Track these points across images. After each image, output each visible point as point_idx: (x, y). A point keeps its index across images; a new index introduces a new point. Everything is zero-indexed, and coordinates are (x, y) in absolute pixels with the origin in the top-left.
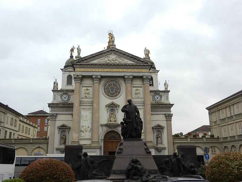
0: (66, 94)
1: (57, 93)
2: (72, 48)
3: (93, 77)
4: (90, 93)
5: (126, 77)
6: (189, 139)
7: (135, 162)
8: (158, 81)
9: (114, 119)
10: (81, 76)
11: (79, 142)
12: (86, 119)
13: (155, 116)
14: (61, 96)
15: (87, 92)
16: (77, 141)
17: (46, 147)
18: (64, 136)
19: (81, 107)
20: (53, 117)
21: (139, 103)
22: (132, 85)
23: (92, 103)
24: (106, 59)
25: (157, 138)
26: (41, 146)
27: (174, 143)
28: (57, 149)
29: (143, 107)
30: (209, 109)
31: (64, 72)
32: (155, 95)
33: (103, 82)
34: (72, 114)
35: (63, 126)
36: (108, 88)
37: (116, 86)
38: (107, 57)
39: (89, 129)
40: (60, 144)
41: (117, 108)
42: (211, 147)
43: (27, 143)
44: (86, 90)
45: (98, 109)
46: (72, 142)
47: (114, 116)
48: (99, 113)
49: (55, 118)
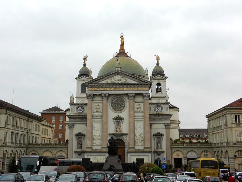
0: (81, 107)
2: (85, 57)
3: (102, 95)
4: (100, 108)
5: (129, 95)
6: (185, 145)
7: (112, 166)
8: (165, 86)
9: (119, 130)
10: (92, 95)
11: (92, 147)
12: (97, 129)
13: (157, 125)
14: (77, 109)
15: (98, 107)
16: (90, 147)
17: (67, 150)
18: (81, 142)
19: (93, 120)
21: (140, 116)
22: (135, 101)
23: (102, 116)
24: (113, 80)
25: (157, 144)
26: (62, 149)
28: (75, 152)
29: (143, 119)
30: (208, 117)
31: (78, 81)
33: (110, 99)
34: (86, 124)
35: (80, 133)
36: (114, 104)
37: (120, 101)
38: (114, 78)
39: (100, 137)
40: (77, 149)
41: (122, 120)
42: (204, 151)
43: (52, 147)
44: (97, 105)
45: (107, 122)
46: (87, 147)
47: (120, 127)
48: (107, 125)
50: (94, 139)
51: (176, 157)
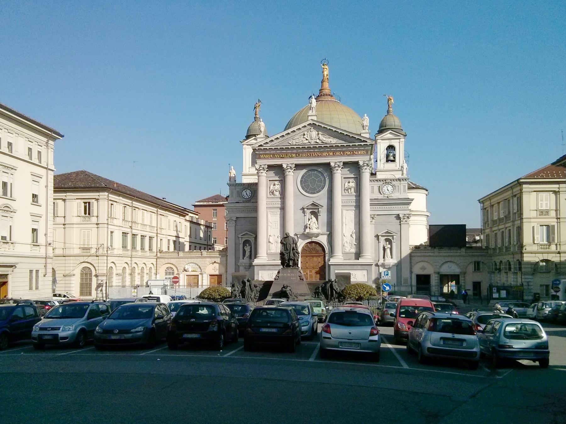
32: (383, 186)
36: (305, 182)
50: (269, 242)
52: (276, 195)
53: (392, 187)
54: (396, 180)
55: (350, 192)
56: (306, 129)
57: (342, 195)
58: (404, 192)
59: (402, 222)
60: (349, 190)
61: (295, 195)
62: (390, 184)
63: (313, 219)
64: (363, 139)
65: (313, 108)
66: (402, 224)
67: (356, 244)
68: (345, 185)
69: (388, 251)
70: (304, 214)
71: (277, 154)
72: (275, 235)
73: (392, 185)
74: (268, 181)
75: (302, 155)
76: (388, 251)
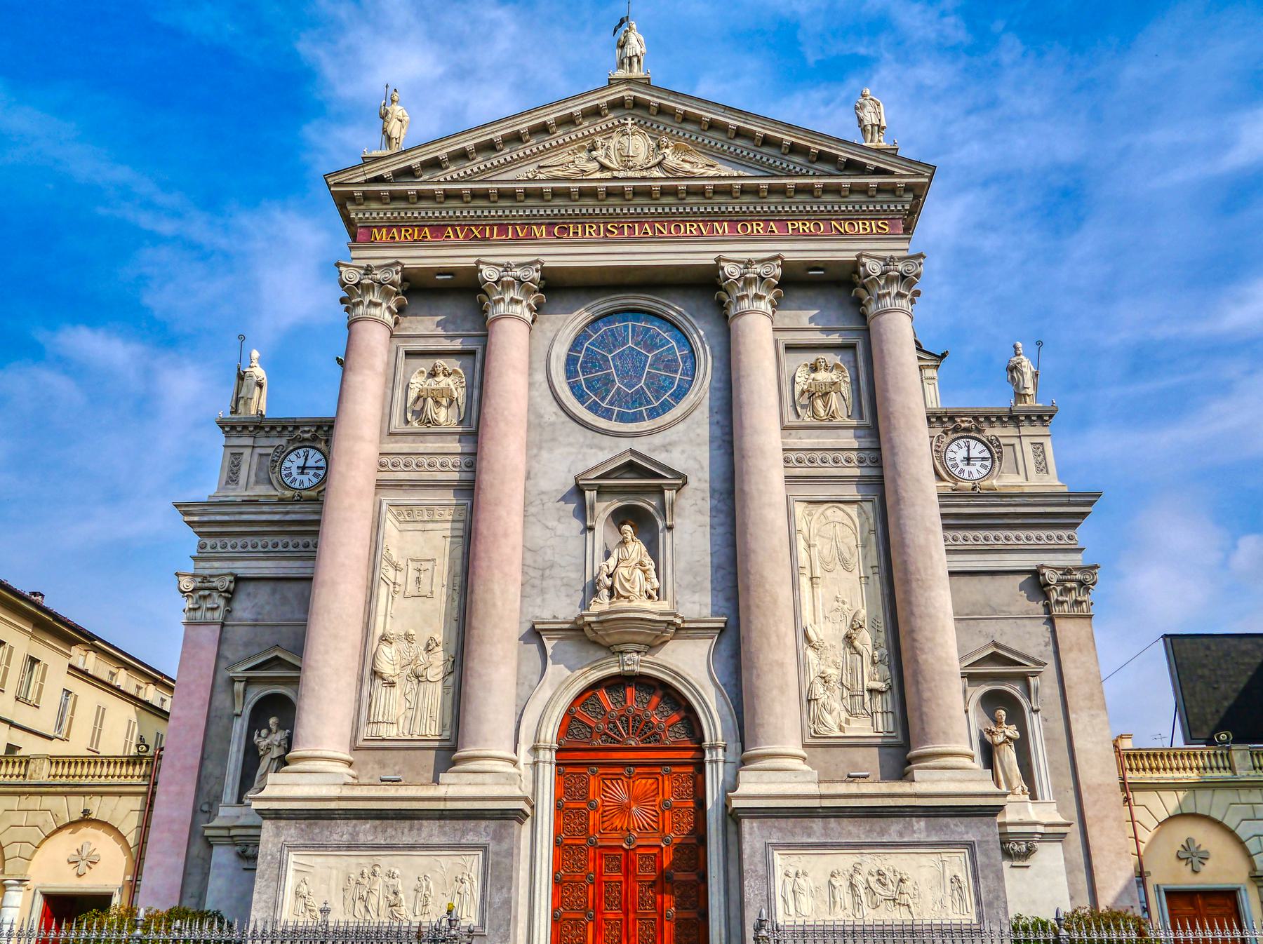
1: (249, 441)
20: (205, 597)
26: (101, 807)
27: (1124, 786)
36: (593, 362)
49: (222, 602)
50: (375, 674)
51: (1185, 879)
52: (436, 423)
53: (984, 448)
54: (999, 418)
55: (822, 413)
56: (601, 124)
57: (784, 428)
58: (1039, 470)
59: (1056, 610)
60: (819, 403)
61: (535, 423)
62: (973, 434)
63: (631, 546)
64: (872, 164)
65: (630, 58)
66: (1060, 617)
67: (880, 685)
68: (797, 379)
69: (1009, 756)
70: (585, 520)
71: (453, 226)
72: (412, 632)
73: (985, 440)
74: (401, 354)
75: (580, 231)
76: (1009, 756)
